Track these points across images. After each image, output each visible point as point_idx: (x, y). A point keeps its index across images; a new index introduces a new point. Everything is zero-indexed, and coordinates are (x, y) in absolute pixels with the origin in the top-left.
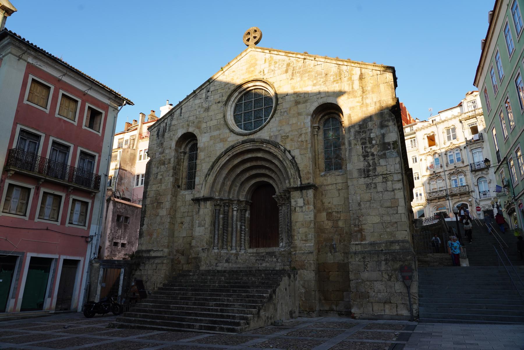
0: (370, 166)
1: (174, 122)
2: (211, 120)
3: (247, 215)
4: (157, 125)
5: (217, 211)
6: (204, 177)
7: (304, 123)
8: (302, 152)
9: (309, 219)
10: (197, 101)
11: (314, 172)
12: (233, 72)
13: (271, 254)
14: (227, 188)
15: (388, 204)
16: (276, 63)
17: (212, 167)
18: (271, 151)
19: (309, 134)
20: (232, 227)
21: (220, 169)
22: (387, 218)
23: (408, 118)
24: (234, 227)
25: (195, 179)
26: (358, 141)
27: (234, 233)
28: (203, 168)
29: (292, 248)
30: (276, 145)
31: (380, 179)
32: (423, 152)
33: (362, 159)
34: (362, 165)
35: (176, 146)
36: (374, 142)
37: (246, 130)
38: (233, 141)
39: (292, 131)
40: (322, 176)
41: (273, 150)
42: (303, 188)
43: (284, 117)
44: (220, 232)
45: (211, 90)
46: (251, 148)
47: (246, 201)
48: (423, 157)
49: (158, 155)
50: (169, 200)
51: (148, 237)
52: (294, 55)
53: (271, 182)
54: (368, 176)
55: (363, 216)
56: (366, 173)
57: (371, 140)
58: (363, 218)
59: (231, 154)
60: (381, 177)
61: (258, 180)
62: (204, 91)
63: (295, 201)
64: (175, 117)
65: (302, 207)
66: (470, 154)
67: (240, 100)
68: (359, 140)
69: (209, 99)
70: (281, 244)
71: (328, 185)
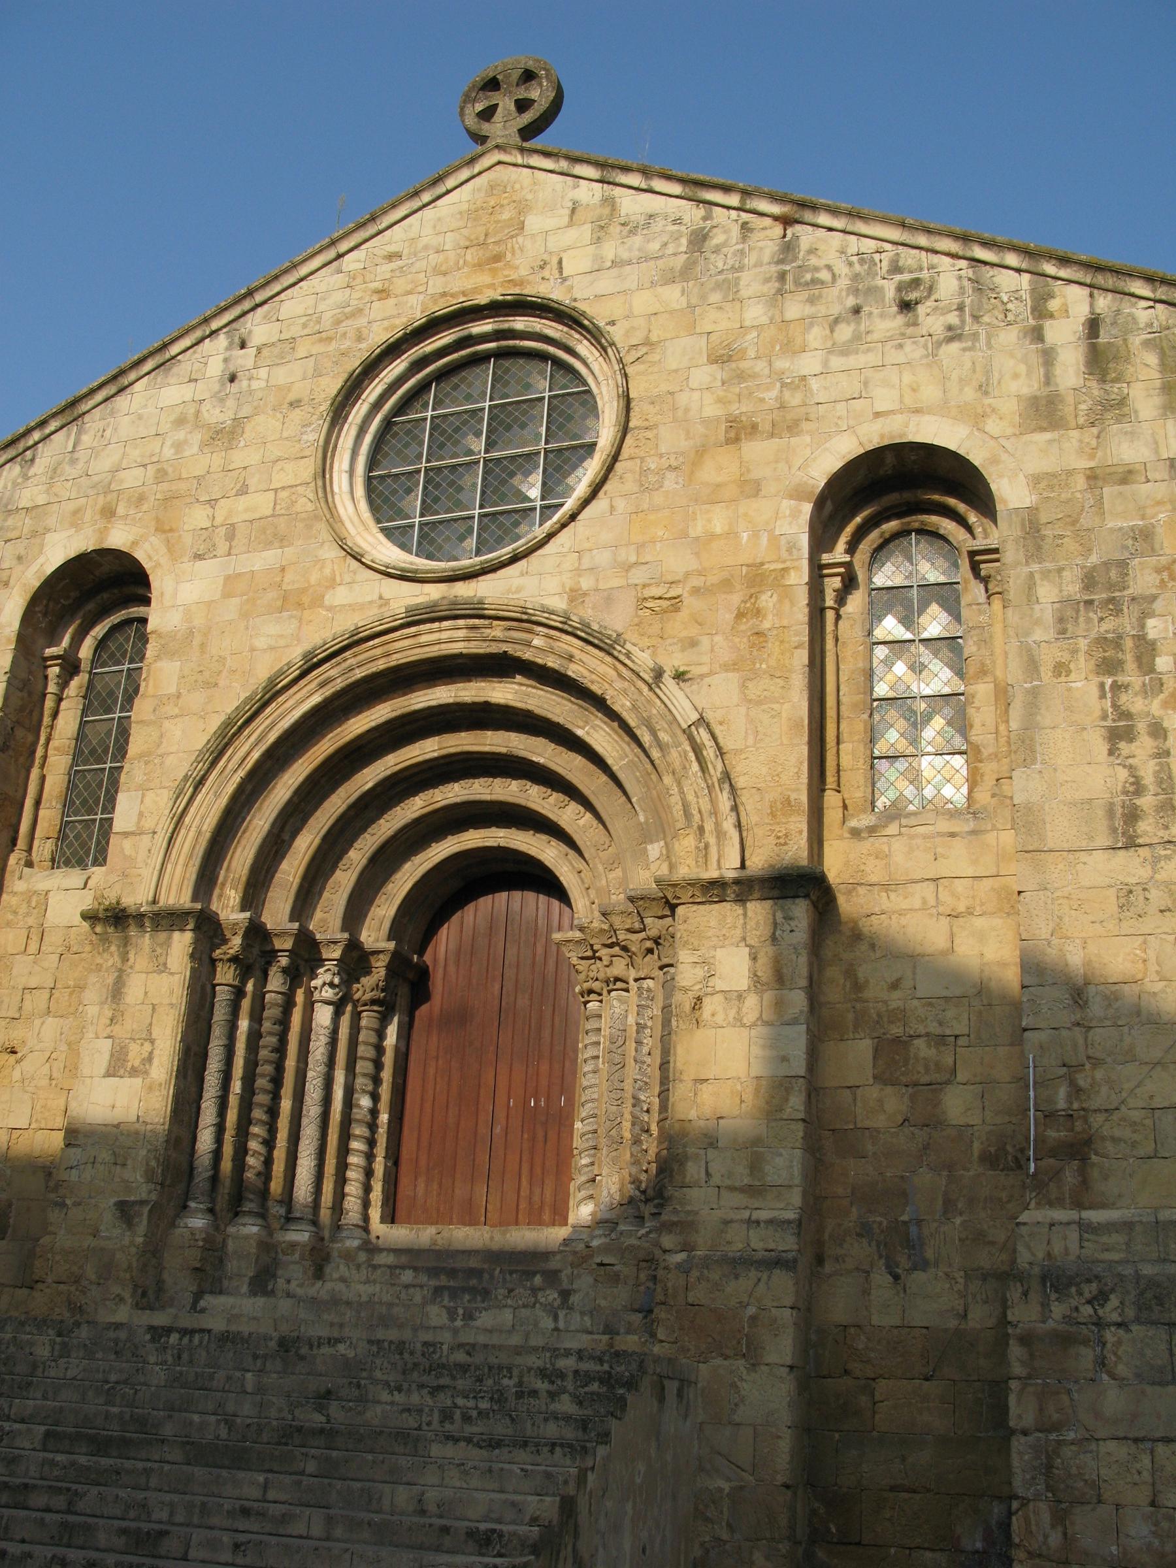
2: (243, 491)
16: (631, 228)
21: (269, 754)
25: (111, 801)
26: (1074, 652)
29: (668, 1227)
33: (1100, 747)
36: (1163, 663)
37: (430, 557)
38: (353, 607)
40: (855, 833)
41: (587, 666)
43: (658, 498)
45: (256, 340)
52: (734, 200)
54: (1131, 844)
55: (1096, 1062)
57: (1146, 651)
58: (1099, 1074)
62: (222, 340)
64: (39, 467)
65: (740, 997)
68: (1083, 644)
69: (243, 384)
71: (886, 887)
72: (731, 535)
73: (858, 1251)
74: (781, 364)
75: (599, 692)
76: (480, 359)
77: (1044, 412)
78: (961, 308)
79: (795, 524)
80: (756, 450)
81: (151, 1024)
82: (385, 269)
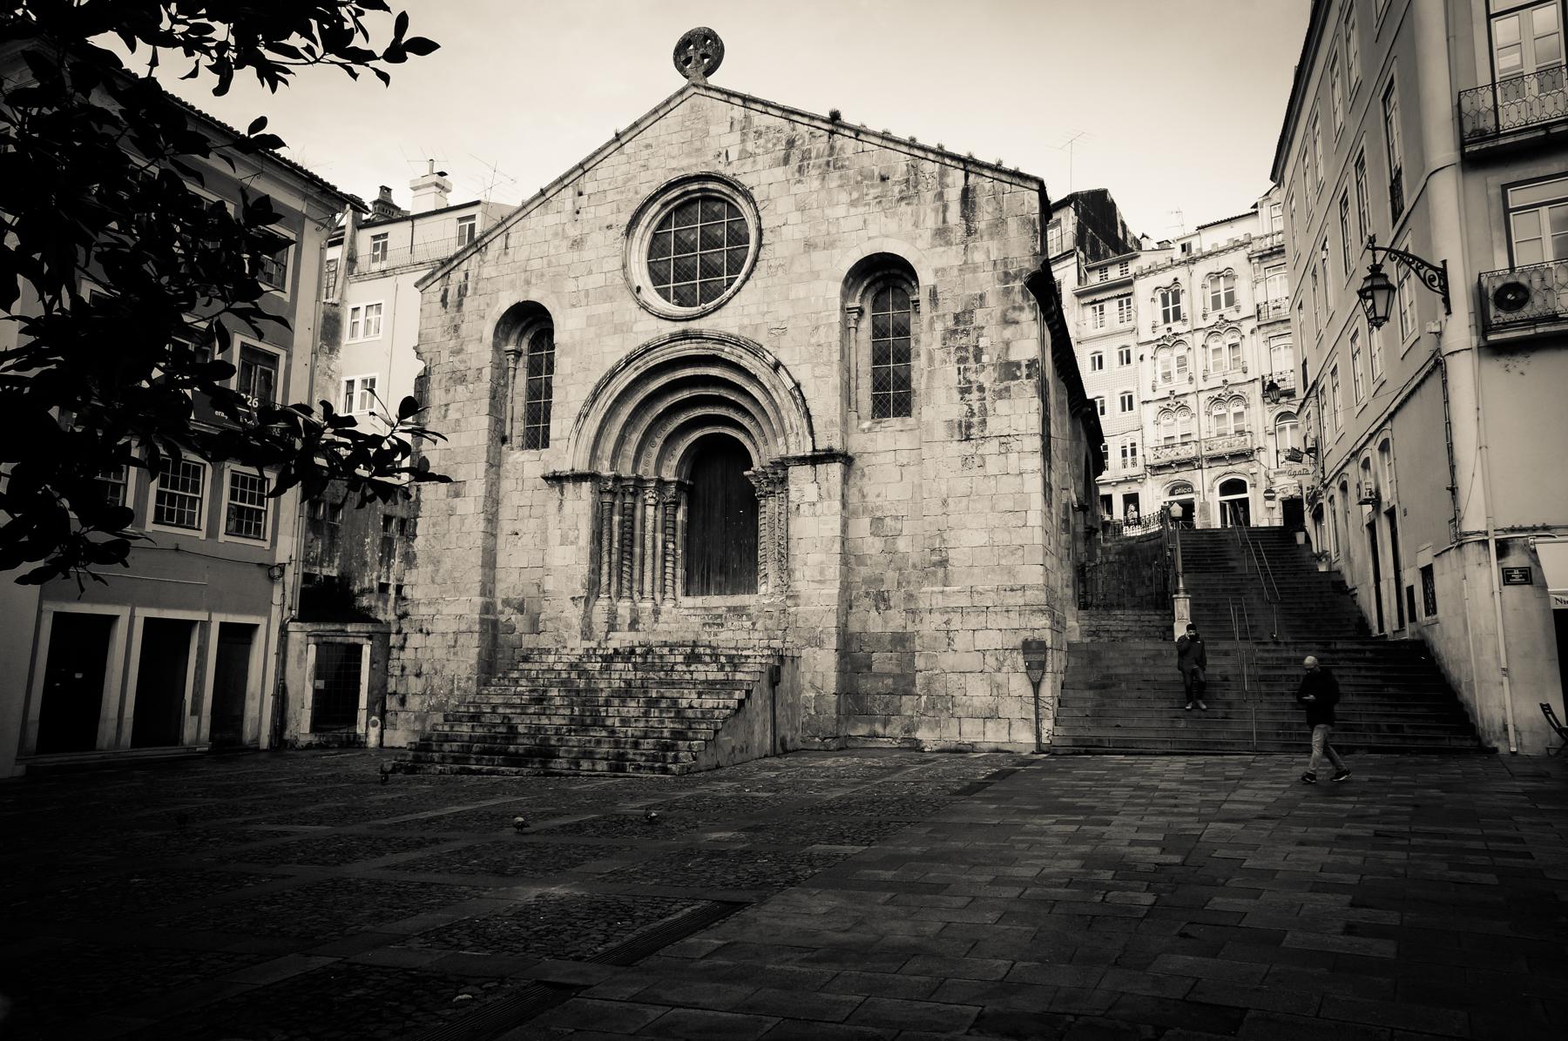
0: (973, 414)
1: (487, 271)
2: (590, 272)
3: (680, 516)
4: (439, 274)
5: (607, 507)
6: (572, 421)
7: (825, 300)
8: (818, 372)
9: (831, 534)
10: (551, 219)
11: (845, 422)
12: (648, 146)
13: (738, 611)
14: (630, 449)
15: (1009, 505)
16: (759, 134)
17: (595, 396)
18: (743, 363)
19: (837, 328)
20: (643, 546)
22: (1001, 537)
23: (1121, 236)
24: (649, 544)
27: (648, 561)
28: (570, 398)
30: (756, 351)
31: (992, 447)
32: (1144, 338)
34: (957, 411)
35: (496, 334)
36: (985, 358)
37: (680, 305)
39: (795, 317)
41: (748, 362)
42: (815, 459)
43: (776, 280)
44: (615, 557)
45: (586, 192)
46: (693, 352)
47: (678, 483)
48: (1148, 351)
49: (445, 357)
50: (482, 474)
51: (430, 568)
52: (806, 120)
53: (741, 437)
54: (968, 439)
56: (965, 430)
57: (978, 353)
59: (642, 365)
60: (996, 442)
61: (708, 431)
62: (569, 192)
66: (1264, 349)
67: (664, 223)
70: (762, 589)
72: (807, 298)
73: (867, 602)
74: (828, 211)
76: (694, 201)
77: (942, 233)
78: (907, 181)
79: (836, 288)
80: (818, 257)
82: (645, 153)
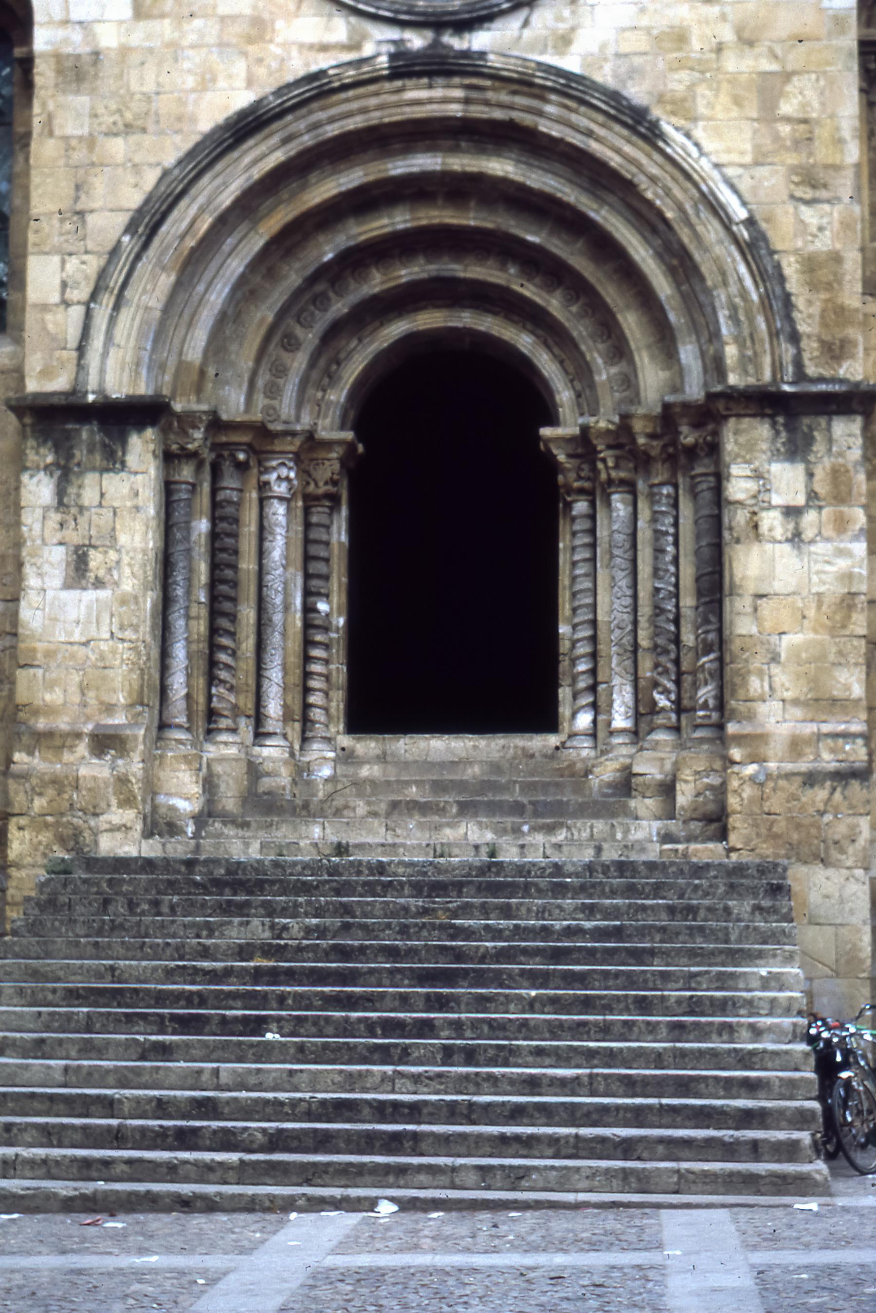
46: (455, 110)
63: (758, 475)
75: (629, 176)
81: (114, 529)
